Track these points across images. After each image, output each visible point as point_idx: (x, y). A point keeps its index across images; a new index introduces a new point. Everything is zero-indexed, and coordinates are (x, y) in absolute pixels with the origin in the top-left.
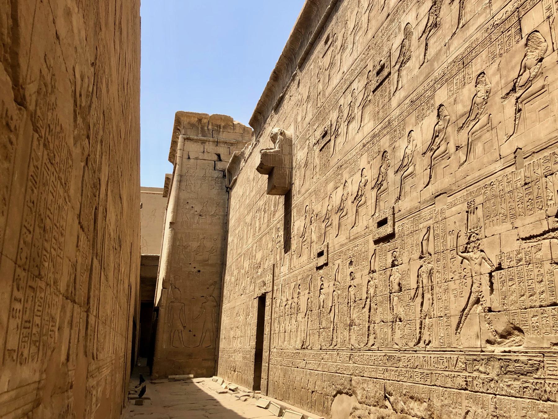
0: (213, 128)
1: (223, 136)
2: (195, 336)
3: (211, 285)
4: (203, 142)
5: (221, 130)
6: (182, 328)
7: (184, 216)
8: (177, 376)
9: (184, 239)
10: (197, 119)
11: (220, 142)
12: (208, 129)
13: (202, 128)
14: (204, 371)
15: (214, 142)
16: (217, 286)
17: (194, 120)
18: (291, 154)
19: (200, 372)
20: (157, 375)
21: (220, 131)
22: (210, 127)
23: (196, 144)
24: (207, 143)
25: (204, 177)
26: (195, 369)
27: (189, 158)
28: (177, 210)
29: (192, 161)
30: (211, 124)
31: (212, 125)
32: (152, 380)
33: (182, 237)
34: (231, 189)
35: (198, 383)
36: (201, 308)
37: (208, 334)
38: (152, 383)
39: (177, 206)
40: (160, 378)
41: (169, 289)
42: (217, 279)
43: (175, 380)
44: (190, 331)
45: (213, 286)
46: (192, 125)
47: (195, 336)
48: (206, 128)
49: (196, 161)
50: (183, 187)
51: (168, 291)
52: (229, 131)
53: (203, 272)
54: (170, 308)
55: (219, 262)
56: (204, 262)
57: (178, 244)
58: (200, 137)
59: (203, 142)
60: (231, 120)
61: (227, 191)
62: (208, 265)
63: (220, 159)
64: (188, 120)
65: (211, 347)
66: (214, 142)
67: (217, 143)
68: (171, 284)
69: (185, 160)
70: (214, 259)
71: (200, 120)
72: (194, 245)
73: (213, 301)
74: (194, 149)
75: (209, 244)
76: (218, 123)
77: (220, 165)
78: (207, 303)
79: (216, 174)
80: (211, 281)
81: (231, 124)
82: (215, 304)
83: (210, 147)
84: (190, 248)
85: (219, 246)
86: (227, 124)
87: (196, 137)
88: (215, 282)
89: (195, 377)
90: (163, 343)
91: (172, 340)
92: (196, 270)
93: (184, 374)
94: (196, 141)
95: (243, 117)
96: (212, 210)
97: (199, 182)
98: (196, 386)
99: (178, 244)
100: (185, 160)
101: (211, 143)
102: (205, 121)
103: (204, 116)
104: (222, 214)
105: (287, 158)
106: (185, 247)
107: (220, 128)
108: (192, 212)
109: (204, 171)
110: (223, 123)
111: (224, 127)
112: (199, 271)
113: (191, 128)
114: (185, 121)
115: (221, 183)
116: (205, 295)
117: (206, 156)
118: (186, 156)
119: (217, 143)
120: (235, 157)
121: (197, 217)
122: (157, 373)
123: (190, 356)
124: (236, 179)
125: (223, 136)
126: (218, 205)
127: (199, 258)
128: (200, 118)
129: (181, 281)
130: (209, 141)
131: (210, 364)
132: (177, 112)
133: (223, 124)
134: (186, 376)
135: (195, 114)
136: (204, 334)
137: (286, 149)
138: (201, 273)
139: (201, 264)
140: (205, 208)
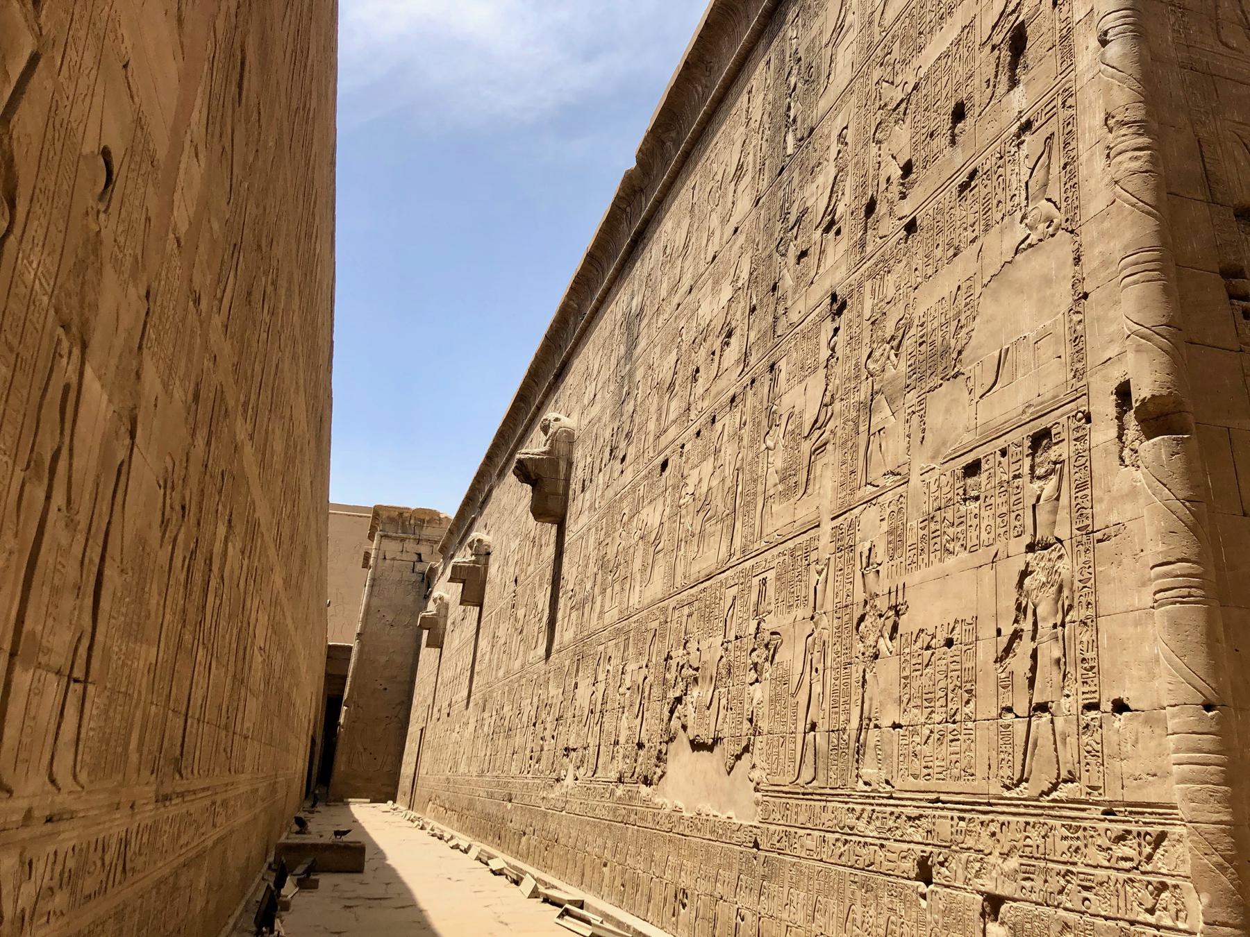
1: (427, 532)
4: (403, 540)
13: (403, 523)
18: (446, 617)
19: (378, 797)
25: (400, 581)
40: (335, 801)
46: (391, 520)
50: (376, 593)
59: (403, 540)
60: (438, 514)
63: (420, 560)
67: (419, 541)
69: (380, 561)
71: (401, 514)
72: (383, 659)
74: (392, 547)
77: (419, 567)
79: (414, 577)
83: (410, 546)
90: (341, 764)
95: (449, 508)
100: (380, 561)
105: (441, 623)
110: (426, 518)
113: (391, 523)
114: (384, 515)
117: (405, 556)
118: (381, 557)
120: (431, 568)
123: (369, 780)
131: (389, 789)
137: (443, 612)
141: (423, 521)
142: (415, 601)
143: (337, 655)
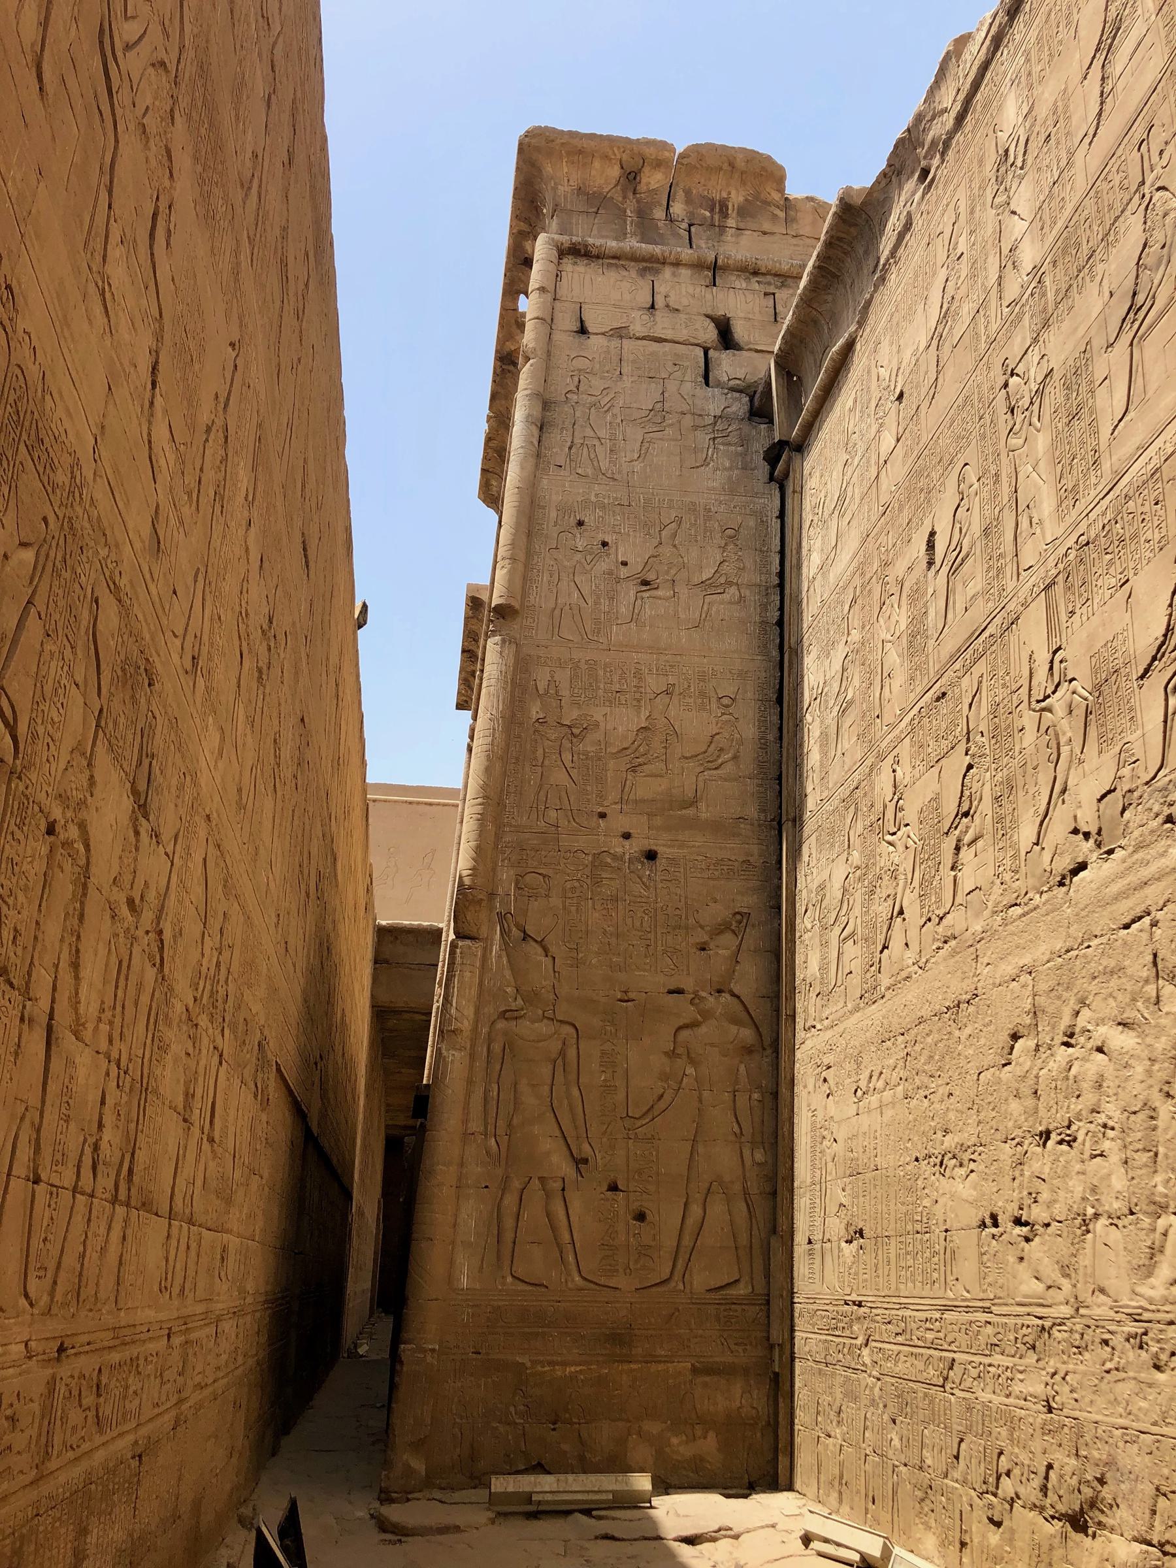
0: (691, 215)
2: (641, 1217)
3: (723, 928)
5: (731, 222)
6: (567, 1169)
7: (563, 585)
8: (545, 1485)
9: (565, 693)
10: (615, 172)
11: (726, 268)
12: (670, 218)
13: (643, 214)
14: (709, 1445)
15: (698, 266)
16: (753, 937)
17: (605, 176)
19: (680, 1447)
20: (418, 1465)
21: (723, 228)
22: (678, 209)
23: (613, 275)
24: (667, 272)
25: (658, 415)
26: (653, 1427)
27: (583, 331)
28: (529, 553)
29: (595, 343)
30: (680, 195)
31: (689, 200)
32: (386, 1497)
33: (552, 681)
34: (800, 447)
35: (691, 1541)
36: (672, 1054)
37: (717, 1208)
38: (384, 1526)
39: (529, 534)
40: (434, 1482)
41: (488, 942)
42: (748, 901)
43: (536, 1511)
44: (614, 1188)
45: (728, 939)
46: (595, 202)
47: (641, 1217)
48: (659, 214)
49: (615, 343)
51: (486, 951)
52: (767, 226)
53: (673, 861)
54: (497, 1047)
55: (752, 811)
56: (678, 809)
57: (535, 711)
58: (632, 244)
59: (650, 265)
61: (771, 478)
62: (694, 824)
64: (576, 177)
65: (742, 1290)
66: (698, 266)
67: (714, 271)
68: (502, 917)
70: (731, 794)
71: (631, 177)
72: (621, 723)
73: (735, 1021)
74: (606, 294)
75: (695, 724)
76: (717, 188)
78: (703, 1029)
79: (714, 402)
80: (716, 913)
81: (776, 196)
82: (747, 1034)
83: (680, 288)
84: (598, 735)
85: (750, 731)
86: (757, 197)
87: (612, 245)
88: (742, 917)
89: (664, 1486)
91: (508, 1236)
92: (633, 848)
93: (585, 1467)
94: (617, 259)
96: (706, 561)
97: (635, 434)
98: (671, 1555)
99: (535, 711)
101: (685, 272)
102: (653, 180)
103: (649, 152)
104: (756, 578)
106: (575, 732)
107: (724, 214)
108: (603, 565)
109: (654, 390)
111: (743, 212)
112: (651, 856)
114: (562, 180)
115: (744, 441)
116: (688, 984)
118: (567, 322)
119: (714, 271)
121: (629, 591)
122: (418, 1446)
123: (618, 1340)
124: (850, 347)
125: (739, 247)
126: (732, 537)
127: (647, 788)
128: (635, 162)
129: (555, 901)
130: (677, 264)
131: (739, 1398)
132: (528, 134)
133: (737, 197)
134: (607, 1483)
135: (610, 139)
136: (696, 1210)
138: (661, 862)
139: (658, 821)
140: (667, 550)
141: (722, 208)
142: (731, 489)
143: (402, 949)
